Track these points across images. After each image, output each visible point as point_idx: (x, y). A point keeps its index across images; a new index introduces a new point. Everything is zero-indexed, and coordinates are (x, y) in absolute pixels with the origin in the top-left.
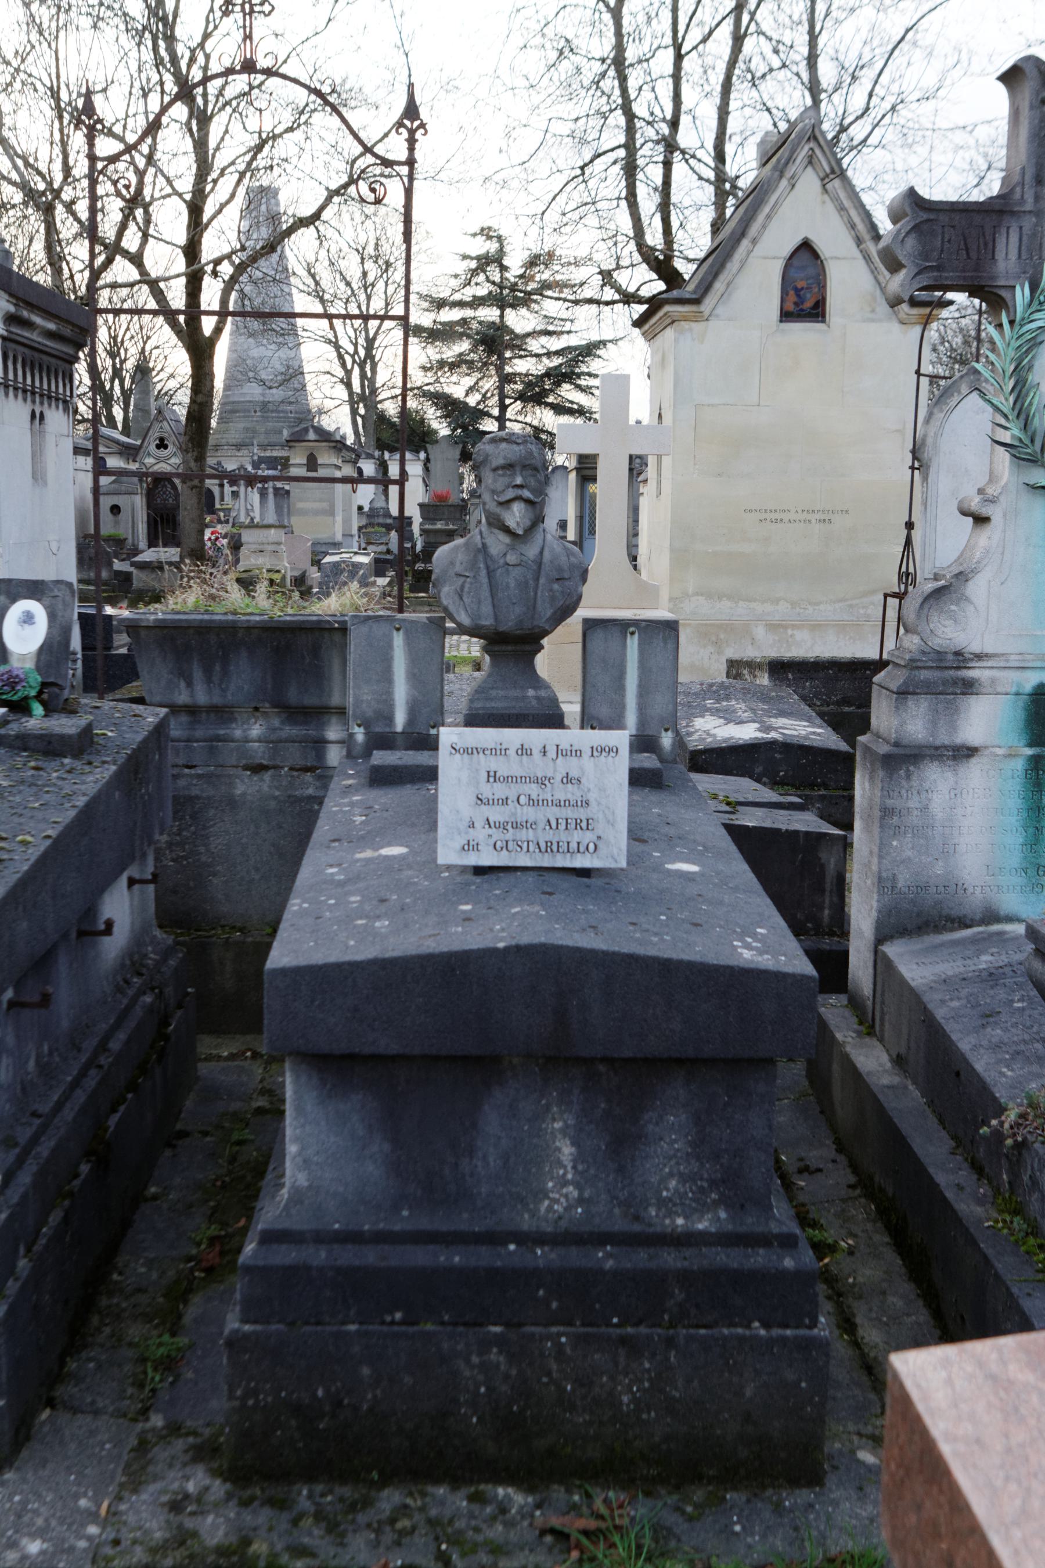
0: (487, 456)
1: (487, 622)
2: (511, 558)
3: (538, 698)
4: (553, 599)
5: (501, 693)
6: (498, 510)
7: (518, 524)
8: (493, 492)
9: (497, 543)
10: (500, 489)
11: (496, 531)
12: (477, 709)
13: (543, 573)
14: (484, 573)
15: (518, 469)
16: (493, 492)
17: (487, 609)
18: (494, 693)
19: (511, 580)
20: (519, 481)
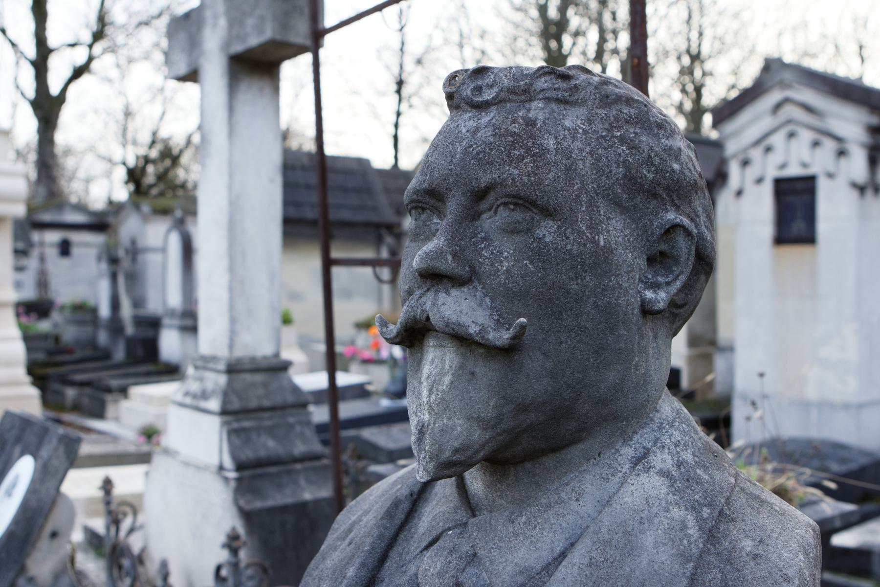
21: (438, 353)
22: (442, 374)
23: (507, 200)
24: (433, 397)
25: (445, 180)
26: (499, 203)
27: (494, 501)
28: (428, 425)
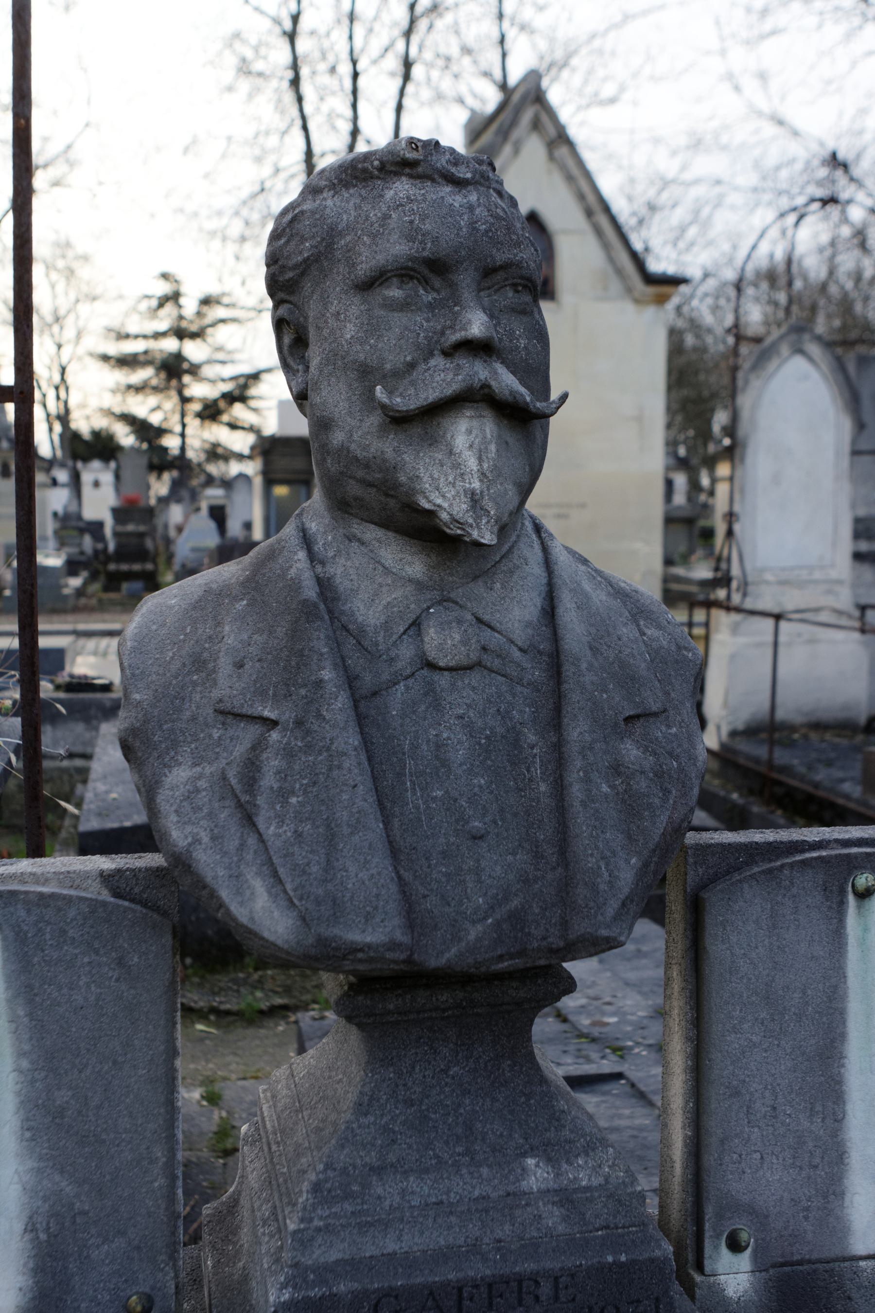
0: (332, 234)
1: (375, 931)
2: (443, 640)
3: (566, 1197)
4: (631, 807)
5: (421, 1189)
6: (388, 447)
7: (475, 500)
8: (367, 374)
9: (379, 578)
10: (393, 360)
11: (371, 533)
12: (325, 1272)
13: (575, 698)
14: (338, 705)
15: (466, 279)
16: (367, 374)
17: (365, 871)
18: (387, 1191)
19: (452, 727)
20: (477, 325)
21: (475, 423)
22: (485, 441)
23: (519, 281)
24: (485, 465)
25: (456, 251)
26: (506, 283)
27: (442, 580)
28: (482, 492)
